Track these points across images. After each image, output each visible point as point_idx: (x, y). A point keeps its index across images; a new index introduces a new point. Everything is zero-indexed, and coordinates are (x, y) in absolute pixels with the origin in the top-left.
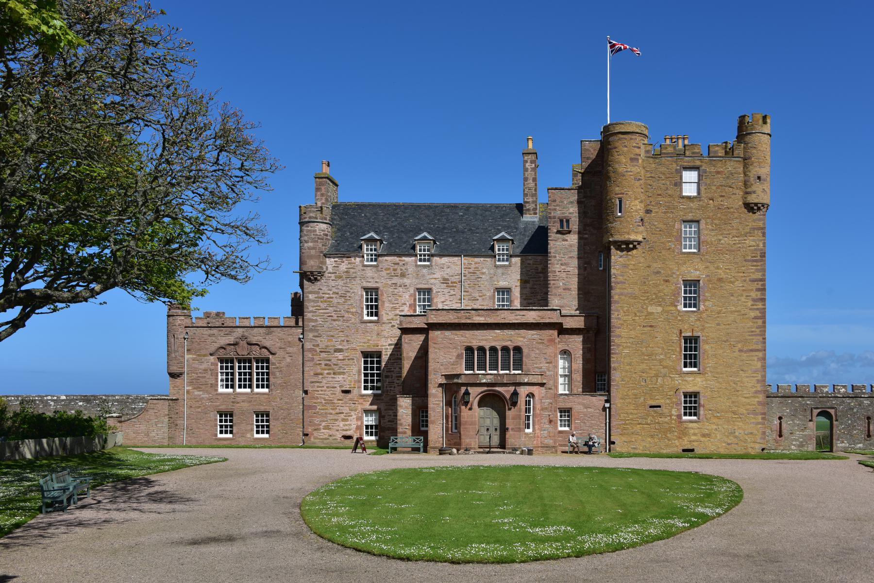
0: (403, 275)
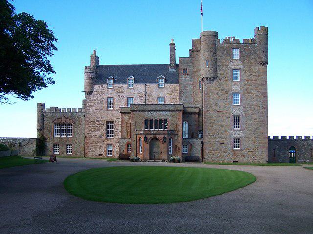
0: (122, 92)
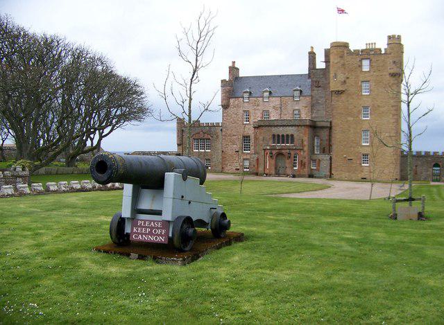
0: (258, 106)
